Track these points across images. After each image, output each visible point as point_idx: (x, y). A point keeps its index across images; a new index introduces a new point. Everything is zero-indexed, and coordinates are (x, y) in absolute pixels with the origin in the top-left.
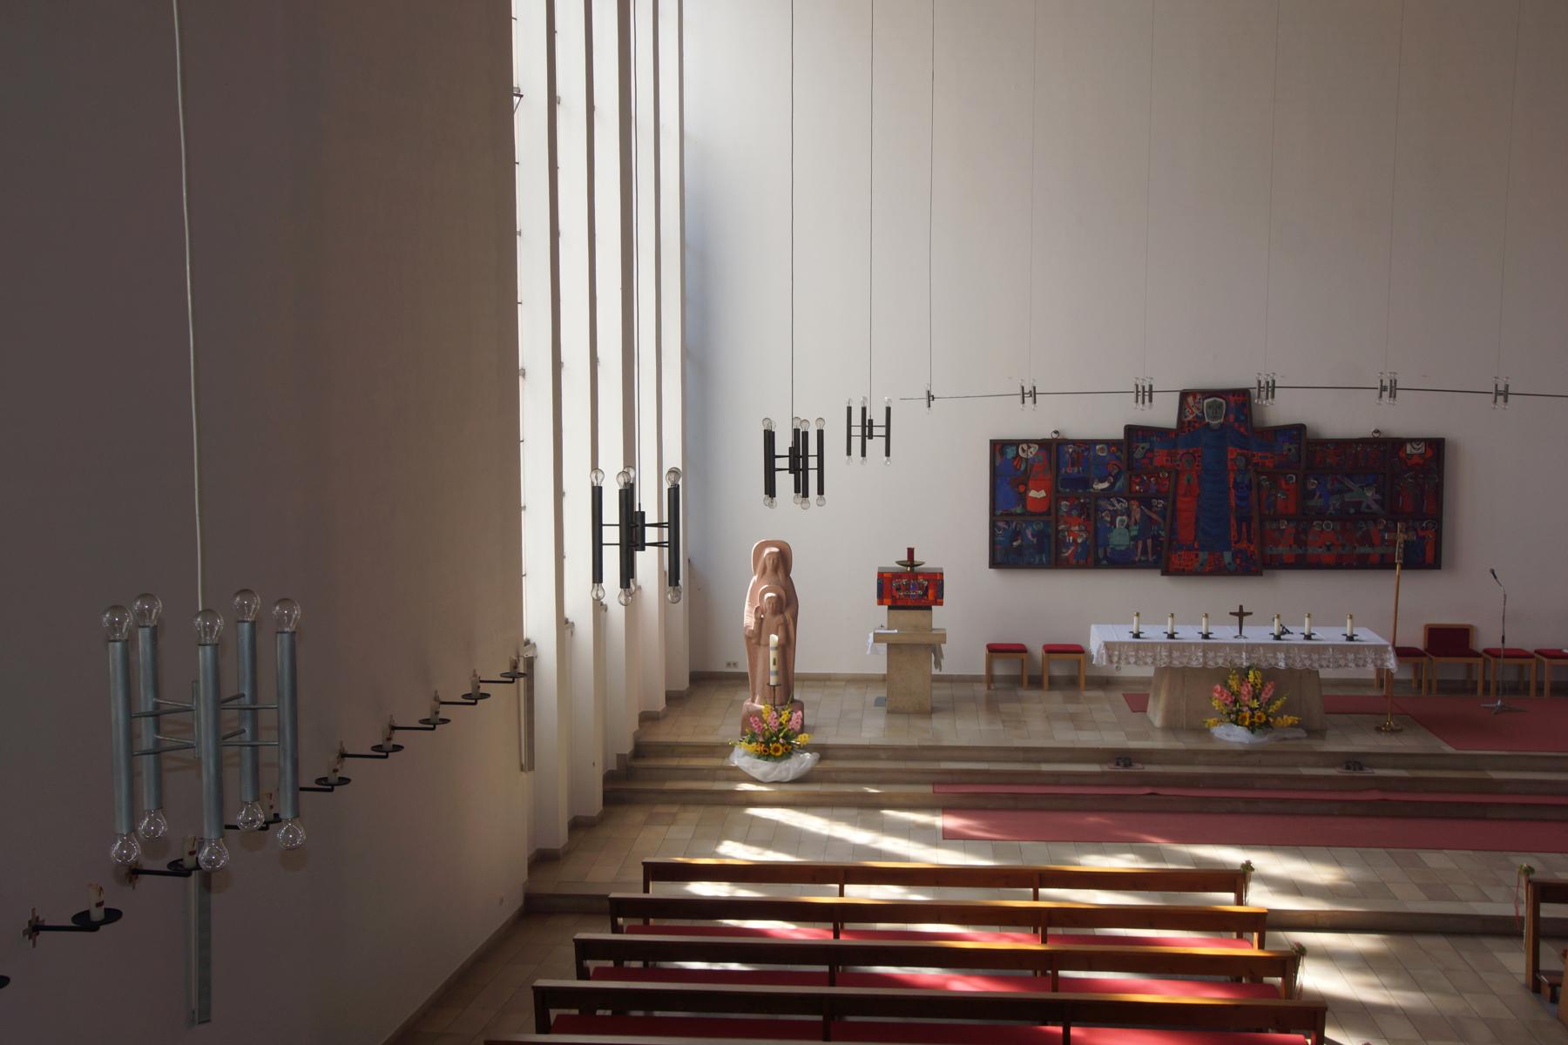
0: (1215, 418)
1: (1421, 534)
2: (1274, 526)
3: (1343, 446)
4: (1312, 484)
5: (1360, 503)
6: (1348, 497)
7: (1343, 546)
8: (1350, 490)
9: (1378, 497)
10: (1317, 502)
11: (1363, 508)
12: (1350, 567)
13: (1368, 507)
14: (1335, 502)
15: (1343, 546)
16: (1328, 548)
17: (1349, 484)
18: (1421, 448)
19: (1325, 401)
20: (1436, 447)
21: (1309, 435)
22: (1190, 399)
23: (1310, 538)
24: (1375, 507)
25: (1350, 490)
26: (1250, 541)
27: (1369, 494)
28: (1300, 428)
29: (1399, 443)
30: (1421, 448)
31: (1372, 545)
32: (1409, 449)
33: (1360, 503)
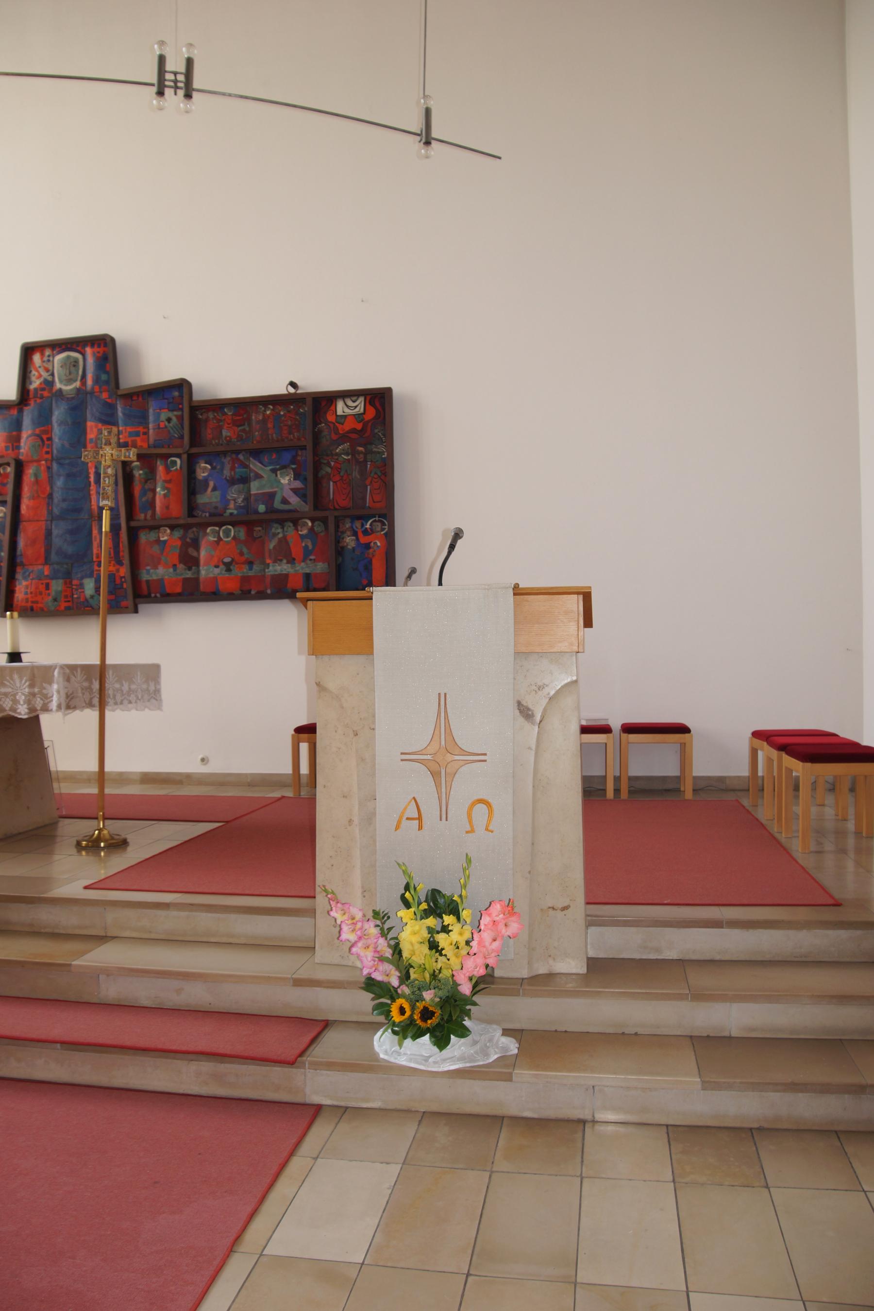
0: (70, 381)
1: (363, 540)
2: (152, 536)
3: (243, 407)
4: (203, 470)
5: (271, 496)
6: (255, 487)
7: (250, 563)
8: (258, 476)
9: (298, 484)
10: (208, 498)
11: (277, 504)
12: (261, 596)
13: (285, 501)
14: (235, 496)
15: (250, 563)
16: (228, 567)
17: (255, 465)
18: (359, 406)
19: (230, 351)
20: (380, 400)
21: (196, 397)
22: (36, 358)
23: (203, 553)
24: (294, 500)
25: (258, 476)
26: (120, 563)
27: (285, 481)
28: (182, 386)
29: (324, 401)
30: (359, 406)
31: (291, 561)
32: (341, 408)
33: (271, 496)
